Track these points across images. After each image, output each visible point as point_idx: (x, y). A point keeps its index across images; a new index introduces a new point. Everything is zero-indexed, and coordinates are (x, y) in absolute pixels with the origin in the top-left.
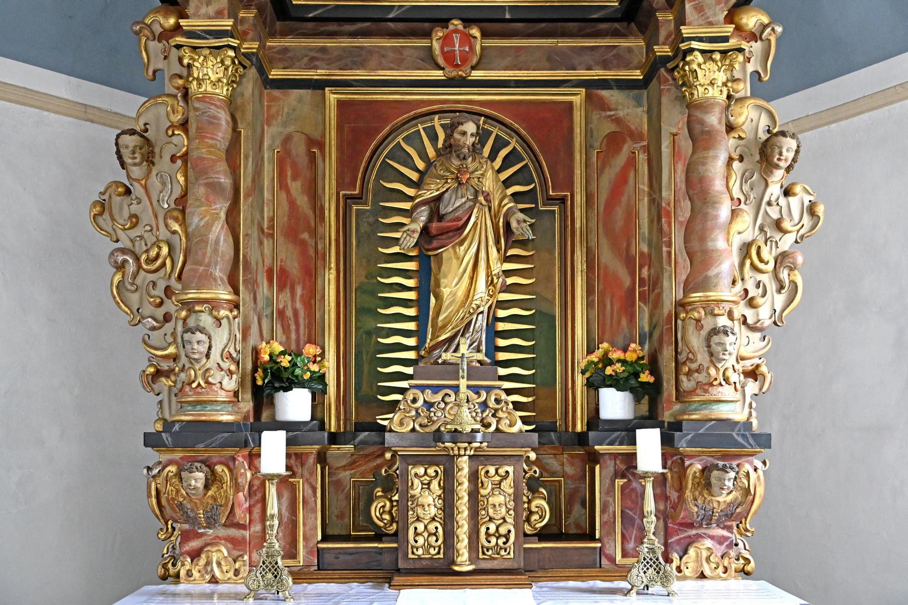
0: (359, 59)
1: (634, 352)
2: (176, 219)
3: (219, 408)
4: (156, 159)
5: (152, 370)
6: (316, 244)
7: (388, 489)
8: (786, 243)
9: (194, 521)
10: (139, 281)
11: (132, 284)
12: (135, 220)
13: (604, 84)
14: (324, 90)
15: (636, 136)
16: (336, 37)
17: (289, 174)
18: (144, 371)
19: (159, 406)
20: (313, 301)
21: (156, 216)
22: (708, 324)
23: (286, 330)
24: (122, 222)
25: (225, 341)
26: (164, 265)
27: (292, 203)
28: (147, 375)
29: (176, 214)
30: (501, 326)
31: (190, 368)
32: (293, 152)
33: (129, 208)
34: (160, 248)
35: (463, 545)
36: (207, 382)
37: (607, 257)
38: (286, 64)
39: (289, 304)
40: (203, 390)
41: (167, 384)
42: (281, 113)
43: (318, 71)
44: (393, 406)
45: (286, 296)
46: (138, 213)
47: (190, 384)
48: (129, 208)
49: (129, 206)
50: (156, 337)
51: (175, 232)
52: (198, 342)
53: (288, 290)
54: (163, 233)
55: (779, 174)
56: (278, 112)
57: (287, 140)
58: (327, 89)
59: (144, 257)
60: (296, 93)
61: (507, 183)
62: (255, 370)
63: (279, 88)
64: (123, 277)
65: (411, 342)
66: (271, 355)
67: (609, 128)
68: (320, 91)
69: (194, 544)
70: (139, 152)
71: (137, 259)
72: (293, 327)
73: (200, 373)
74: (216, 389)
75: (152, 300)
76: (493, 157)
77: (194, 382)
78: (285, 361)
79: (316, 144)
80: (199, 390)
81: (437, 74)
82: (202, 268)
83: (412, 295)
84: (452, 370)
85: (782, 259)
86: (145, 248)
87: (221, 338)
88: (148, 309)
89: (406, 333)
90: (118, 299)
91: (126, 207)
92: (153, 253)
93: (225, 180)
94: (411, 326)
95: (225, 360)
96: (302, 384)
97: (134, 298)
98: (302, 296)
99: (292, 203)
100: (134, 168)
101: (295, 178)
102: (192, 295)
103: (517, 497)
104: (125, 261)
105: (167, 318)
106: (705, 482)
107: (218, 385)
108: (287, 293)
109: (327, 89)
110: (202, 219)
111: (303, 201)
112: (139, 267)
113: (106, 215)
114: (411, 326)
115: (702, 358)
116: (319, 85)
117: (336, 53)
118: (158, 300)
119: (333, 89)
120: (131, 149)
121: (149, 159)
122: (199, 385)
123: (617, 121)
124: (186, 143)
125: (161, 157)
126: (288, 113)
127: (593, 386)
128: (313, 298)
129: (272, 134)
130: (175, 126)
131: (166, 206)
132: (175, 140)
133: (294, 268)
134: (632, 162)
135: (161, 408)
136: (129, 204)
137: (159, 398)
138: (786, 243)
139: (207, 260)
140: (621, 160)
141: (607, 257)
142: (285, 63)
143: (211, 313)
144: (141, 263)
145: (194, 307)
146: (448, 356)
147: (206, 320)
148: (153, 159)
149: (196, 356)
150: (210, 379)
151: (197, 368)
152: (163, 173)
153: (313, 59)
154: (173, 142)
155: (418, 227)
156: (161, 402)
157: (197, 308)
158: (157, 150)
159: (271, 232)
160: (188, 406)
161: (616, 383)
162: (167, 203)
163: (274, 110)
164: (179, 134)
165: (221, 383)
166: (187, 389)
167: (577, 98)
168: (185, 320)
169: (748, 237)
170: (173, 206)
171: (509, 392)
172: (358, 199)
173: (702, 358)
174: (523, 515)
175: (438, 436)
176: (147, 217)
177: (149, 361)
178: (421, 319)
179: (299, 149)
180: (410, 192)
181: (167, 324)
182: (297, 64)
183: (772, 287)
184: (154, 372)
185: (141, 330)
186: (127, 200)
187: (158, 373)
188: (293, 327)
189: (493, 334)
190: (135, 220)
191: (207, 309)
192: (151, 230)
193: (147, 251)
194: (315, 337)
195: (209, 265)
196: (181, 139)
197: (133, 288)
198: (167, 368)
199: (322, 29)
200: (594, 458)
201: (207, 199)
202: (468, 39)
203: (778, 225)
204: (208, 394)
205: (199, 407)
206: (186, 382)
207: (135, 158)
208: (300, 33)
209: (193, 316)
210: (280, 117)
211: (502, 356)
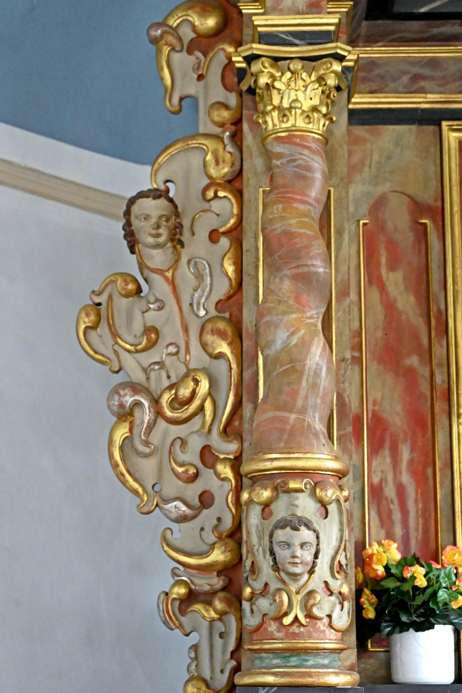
2: (222, 335)
3: (326, 662)
4: (186, 237)
5: (182, 591)
6: (432, 374)
10: (155, 438)
11: (147, 443)
14: (440, 126)
16: (453, 43)
17: (383, 260)
18: (167, 594)
19: (193, 655)
20: (429, 471)
21: (186, 330)
24: (131, 339)
25: (334, 543)
26: (201, 409)
28: (174, 599)
29: (221, 325)
31: (279, 590)
32: (390, 225)
33: (143, 317)
34: (196, 382)
36: (310, 616)
38: (374, 86)
39: (390, 477)
40: (302, 629)
41: (206, 615)
42: (368, 162)
43: (429, 96)
46: (158, 325)
47: (279, 619)
48: (143, 317)
49: (143, 313)
51: (220, 356)
52: (302, 545)
53: (387, 452)
56: (362, 162)
58: (444, 124)
59: (166, 398)
62: (359, 593)
63: (363, 124)
64: (131, 430)
66: (387, 568)
68: (431, 128)
70: (165, 226)
71: (156, 402)
72: (397, 516)
73: (297, 599)
74: (322, 628)
75: (180, 470)
77: (286, 614)
80: (295, 629)
82: (293, 417)
86: (166, 383)
90: (122, 468)
91: (138, 315)
92: (185, 392)
95: (336, 575)
98: (411, 462)
100: (155, 252)
101: (392, 267)
104: (138, 404)
107: (326, 620)
109: (444, 124)
110: (293, 334)
112: (159, 413)
113: (103, 329)
117: (453, 69)
118: (192, 471)
119: (455, 123)
120: (154, 220)
122: (296, 619)
124: (235, 211)
125: (193, 234)
126: (379, 162)
130: (219, 184)
131: (202, 313)
132: (216, 206)
135: (196, 658)
136: (144, 310)
137: (194, 638)
139: (300, 403)
142: (372, 84)
143: (313, 494)
144: (162, 407)
145: (286, 484)
148: (182, 238)
149: (298, 570)
150: (315, 611)
151: (294, 590)
152: (198, 260)
153: (416, 78)
154: (213, 209)
156: (195, 648)
157: (293, 485)
158: (186, 223)
159: (356, 354)
160: (274, 658)
162: (205, 309)
163: (356, 158)
164: (225, 197)
165: (329, 616)
166: (273, 627)
168: (266, 505)
170: (213, 312)
177: (174, 573)
181: (205, 511)
182: (392, 85)
184: (185, 594)
186: (139, 305)
188: (397, 516)
191: (308, 486)
192: (177, 353)
193: (170, 387)
195: (303, 411)
197: (147, 450)
198: (207, 588)
199: (435, 31)
201: (297, 299)
204: (310, 637)
205: (294, 661)
206: (271, 614)
207: (158, 236)
208: (396, 38)
209: (284, 499)
210: (366, 169)
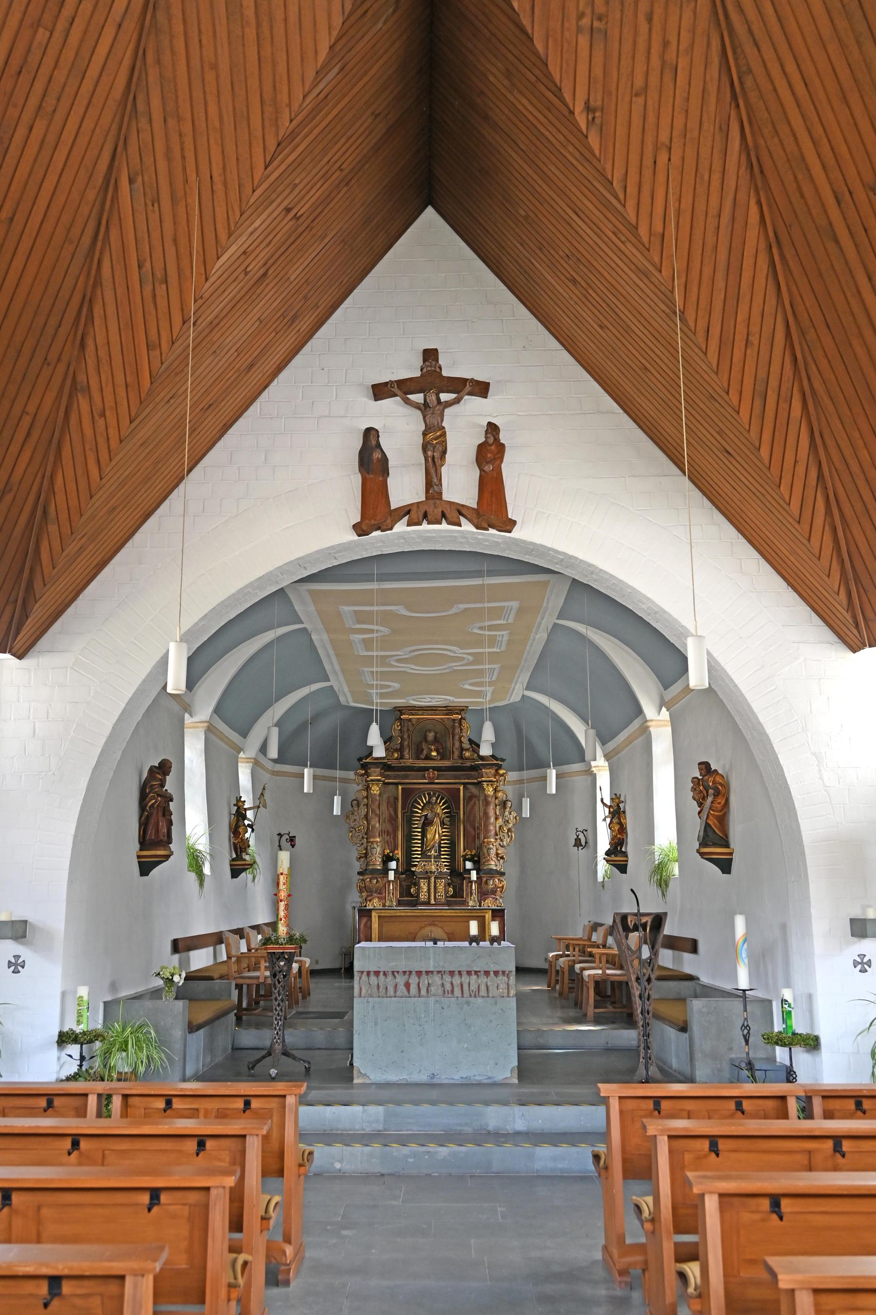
0: (406, 777)
1: (474, 852)
7: (415, 887)
8: (510, 826)
9: (372, 892)
12: (355, 820)
13: (468, 783)
15: (476, 797)
22: (488, 847)
23: (388, 846)
27: (390, 813)
30: (442, 845)
35: (432, 898)
37: (469, 827)
44: (416, 865)
45: (388, 837)
50: (359, 848)
54: (361, 823)
55: (508, 809)
57: (389, 798)
60: (391, 786)
61: (443, 809)
65: (420, 849)
67: (468, 795)
69: (370, 898)
76: (440, 803)
78: (391, 854)
79: (396, 799)
81: (426, 781)
83: (420, 837)
84: (430, 857)
85: (509, 830)
87: (379, 849)
88: (358, 842)
89: (418, 847)
93: (378, 813)
94: (420, 845)
96: (394, 860)
97: (354, 839)
99: (390, 813)
102: (372, 840)
103: (445, 887)
105: (362, 844)
106: (486, 883)
108: (388, 837)
111: (392, 813)
114: (420, 845)
115: (486, 854)
116: (397, 784)
121: (358, 805)
123: (471, 792)
127: (464, 861)
128: (395, 837)
129: (385, 796)
133: (390, 829)
134: (475, 803)
138: (510, 826)
140: (472, 803)
141: (469, 827)
146: (429, 854)
147: (375, 846)
155: (422, 822)
161: (469, 860)
167: (462, 788)
169: (501, 824)
171: (444, 862)
172: (407, 812)
173: (486, 854)
174: (447, 892)
175: (427, 872)
176: (358, 820)
178: (422, 843)
179: (392, 799)
180: (420, 811)
183: (506, 836)
185: (356, 847)
187: (361, 857)
189: (440, 847)
190: (355, 820)
194: (396, 848)
196: (366, 800)
200: (464, 878)
202: (433, 773)
203: (508, 821)
211: (442, 853)
